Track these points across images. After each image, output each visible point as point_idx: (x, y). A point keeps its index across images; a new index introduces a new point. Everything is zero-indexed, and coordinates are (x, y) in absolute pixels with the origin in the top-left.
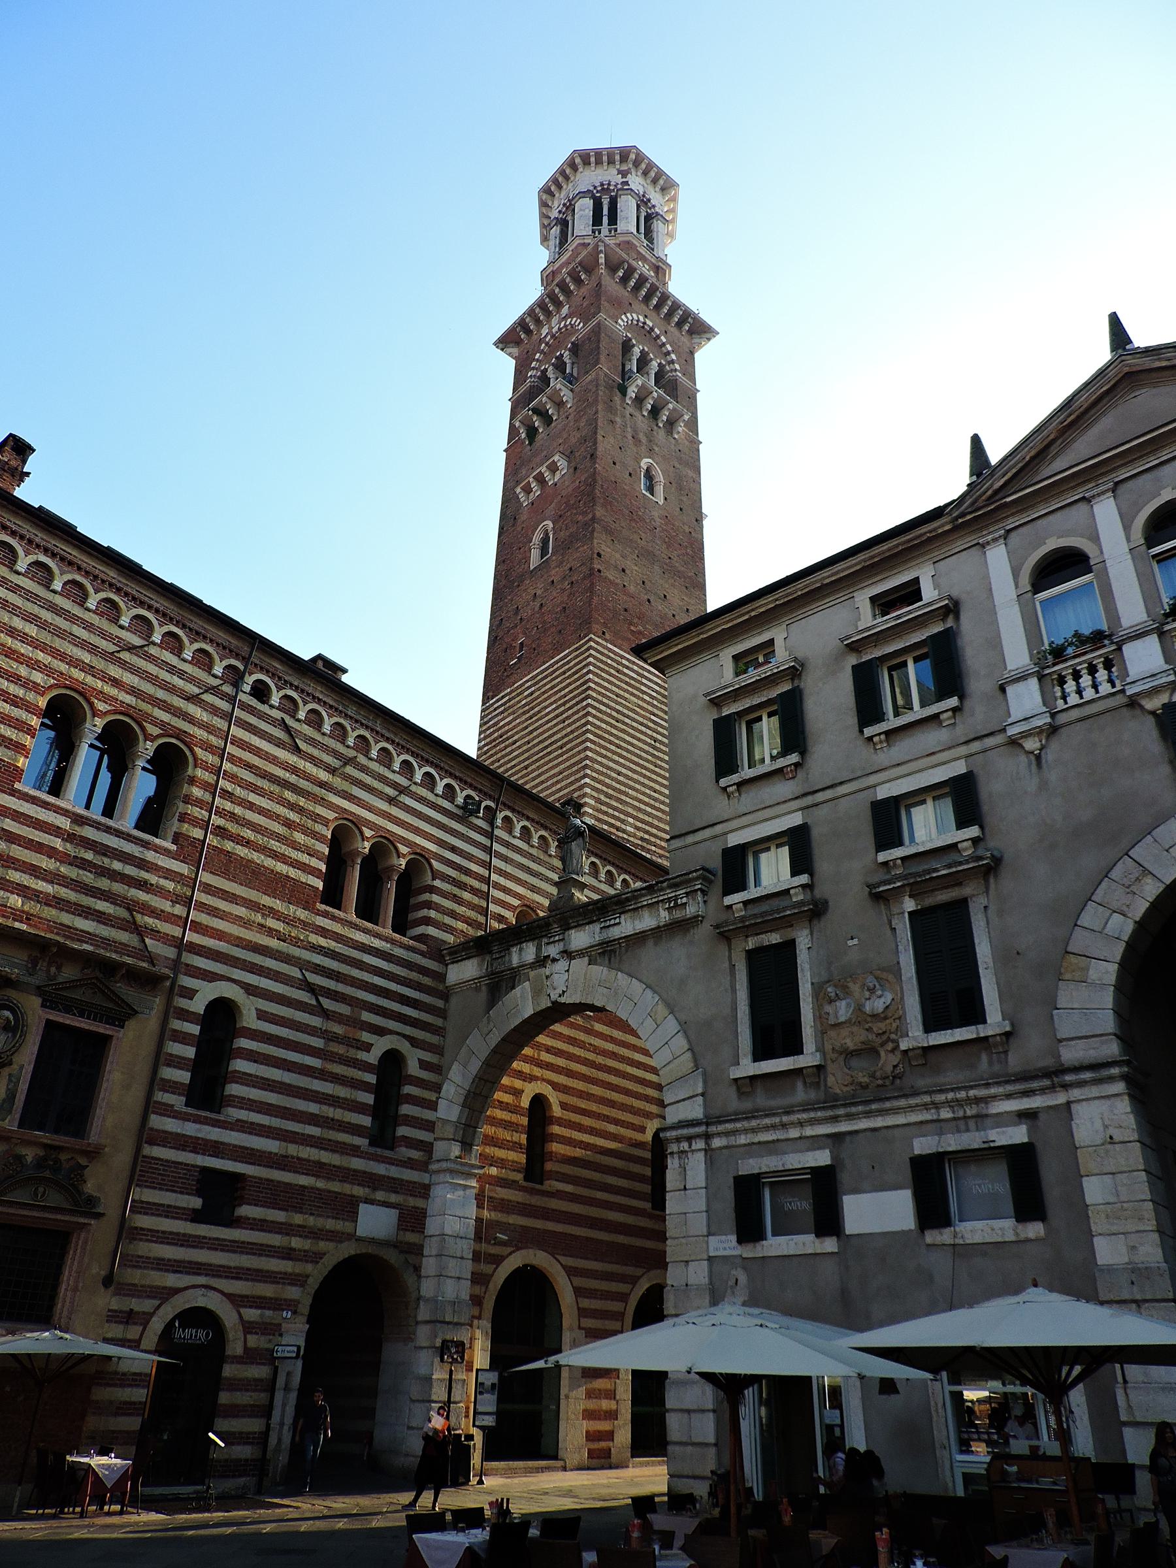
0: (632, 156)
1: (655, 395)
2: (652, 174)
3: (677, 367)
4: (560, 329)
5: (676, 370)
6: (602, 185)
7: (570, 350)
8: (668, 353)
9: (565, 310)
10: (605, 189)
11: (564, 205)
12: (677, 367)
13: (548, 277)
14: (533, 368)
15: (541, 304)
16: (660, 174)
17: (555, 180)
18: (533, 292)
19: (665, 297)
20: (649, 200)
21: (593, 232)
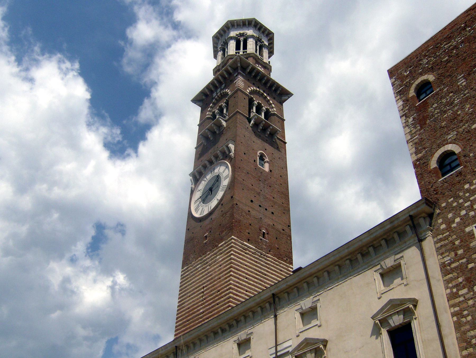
0: (253, 23)
1: (264, 122)
2: (262, 29)
3: (275, 109)
4: (221, 94)
5: (274, 111)
6: (240, 34)
7: (225, 103)
8: (271, 104)
9: (224, 85)
10: (242, 35)
11: (224, 42)
12: (275, 109)
13: (216, 70)
14: (209, 111)
15: (212, 83)
16: (266, 29)
17: (219, 32)
18: (210, 77)
19: (269, 80)
20: (261, 40)
21: (236, 53)
